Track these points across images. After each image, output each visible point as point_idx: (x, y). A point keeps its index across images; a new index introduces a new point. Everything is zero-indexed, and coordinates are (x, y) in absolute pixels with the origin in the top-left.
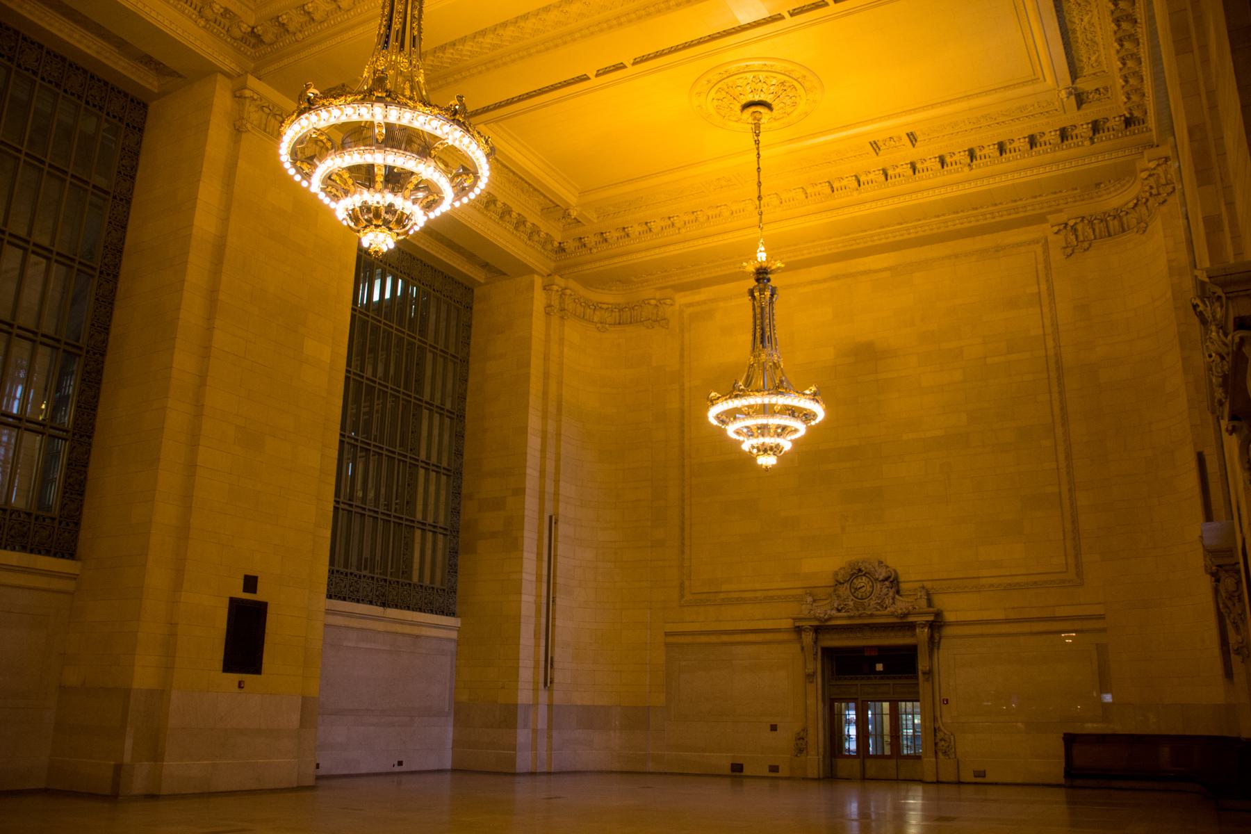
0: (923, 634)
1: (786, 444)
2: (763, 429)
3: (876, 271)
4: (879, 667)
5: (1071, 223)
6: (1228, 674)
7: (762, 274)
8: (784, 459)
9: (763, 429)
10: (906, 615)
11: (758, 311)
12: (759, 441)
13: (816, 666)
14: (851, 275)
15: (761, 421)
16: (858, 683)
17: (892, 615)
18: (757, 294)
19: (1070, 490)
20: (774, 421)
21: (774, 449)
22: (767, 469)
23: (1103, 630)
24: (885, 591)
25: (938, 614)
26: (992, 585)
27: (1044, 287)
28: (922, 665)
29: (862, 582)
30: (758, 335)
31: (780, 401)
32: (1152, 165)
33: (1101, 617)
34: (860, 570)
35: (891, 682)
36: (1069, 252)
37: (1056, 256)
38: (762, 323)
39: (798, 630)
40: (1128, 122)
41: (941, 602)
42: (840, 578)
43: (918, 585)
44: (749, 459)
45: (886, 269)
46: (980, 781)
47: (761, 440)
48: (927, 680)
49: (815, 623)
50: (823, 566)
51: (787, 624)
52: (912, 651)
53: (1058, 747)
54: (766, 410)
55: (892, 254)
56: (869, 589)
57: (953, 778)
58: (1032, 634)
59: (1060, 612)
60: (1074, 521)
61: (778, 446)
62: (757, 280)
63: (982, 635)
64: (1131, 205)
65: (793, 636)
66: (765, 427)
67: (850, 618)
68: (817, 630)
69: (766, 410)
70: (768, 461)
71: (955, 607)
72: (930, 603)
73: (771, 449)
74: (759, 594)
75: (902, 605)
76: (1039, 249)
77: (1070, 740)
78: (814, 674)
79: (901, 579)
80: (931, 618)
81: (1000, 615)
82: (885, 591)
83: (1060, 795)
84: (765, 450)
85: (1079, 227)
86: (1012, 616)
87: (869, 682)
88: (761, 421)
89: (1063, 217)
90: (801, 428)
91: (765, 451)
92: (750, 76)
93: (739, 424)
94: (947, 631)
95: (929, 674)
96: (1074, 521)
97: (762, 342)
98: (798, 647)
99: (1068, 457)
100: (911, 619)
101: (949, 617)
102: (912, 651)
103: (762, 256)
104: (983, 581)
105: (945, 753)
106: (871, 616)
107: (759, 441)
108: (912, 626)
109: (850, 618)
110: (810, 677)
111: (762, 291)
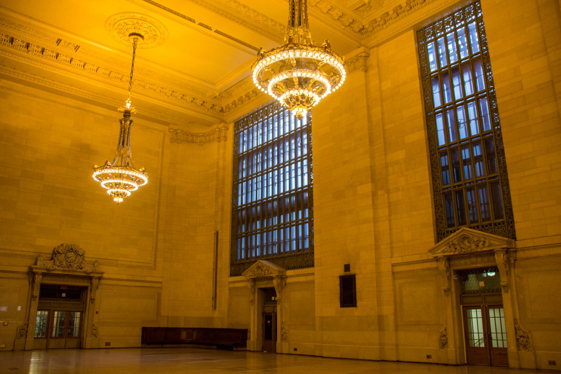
2: (117, 185)
3: (70, 106)
4: (64, 295)
5: (178, 131)
6: (215, 307)
7: (127, 114)
9: (117, 185)
10: (91, 273)
11: (123, 130)
12: (113, 190)
13: (37, 293)
14: (85, 110)
15: (118, 181)
16: (52, 302)
17: (85, 272)
18: (123, 122)
19: (157, 232)
20: (125, 182)
21: (118, 194)
22: (118, 204)
23: (161, 288)
24: (81, 260)
26: (123, 265)
27: (161, 151)
29: (71, 254)
30: (121, 141)
31: (106, 171)
32: (223, 128)
33: (161, 283)
34: (72, 249)
35: (69, 302)
36: (172, 141)
37: (167, 140)
38: (124, 136)
39: (31, 273)
40: (222, 111)
41: (102, 268)
42: (60, 251)
43: (94, 260)
45: (102, 115)
46: (108, 347)
47: (116, 190)
48: (92, 303)
49: (45, 271)
50: (48, 243)
51: (25, 269)
53: (139, 332)
54: (121, 176)
55: (106, 110)
56: (74, 258)
57: (97, 347)
58: (136, 286)
59: (148, 279)
60: (156, 244)
61: (124, 193)
62: (124, 116)
63: (116, 285)
64: (201, 135)
65: (26, 276)
66: (121, 184)
67: (64, 271)
68: (44, 275)
69: (121, 176)
71: (109, 272)
73: (121, 194)
74: (8, 252)
75: (88, 268)
76: (162, 135)
77: (144, 329)
78: (36, 297)
79: (85, 255)
81: (125, 277)
82: (81, 260)
83: (139, 351)
84: (118, 194)
85: (179, 134)
86: (130, 278)
87: (58, 302)
88: (118, 181)
89: (176, 127)
91: (118, 195)
92: (135, 21)
94: (102, 282)
95: (93, 300)
96: (156, 244)
97: (123, 144)
98: (26, 282)
99: (158, 219)
100: (92, 275)
101: (105, 276)
103: (128, 106)
104: (119, 262)
105: (95, 336)
106: (74, 271)
107: (113, 190)
108: (91, 278)
109: (64, 271)
110: (33, 297)
111: (126, 121)
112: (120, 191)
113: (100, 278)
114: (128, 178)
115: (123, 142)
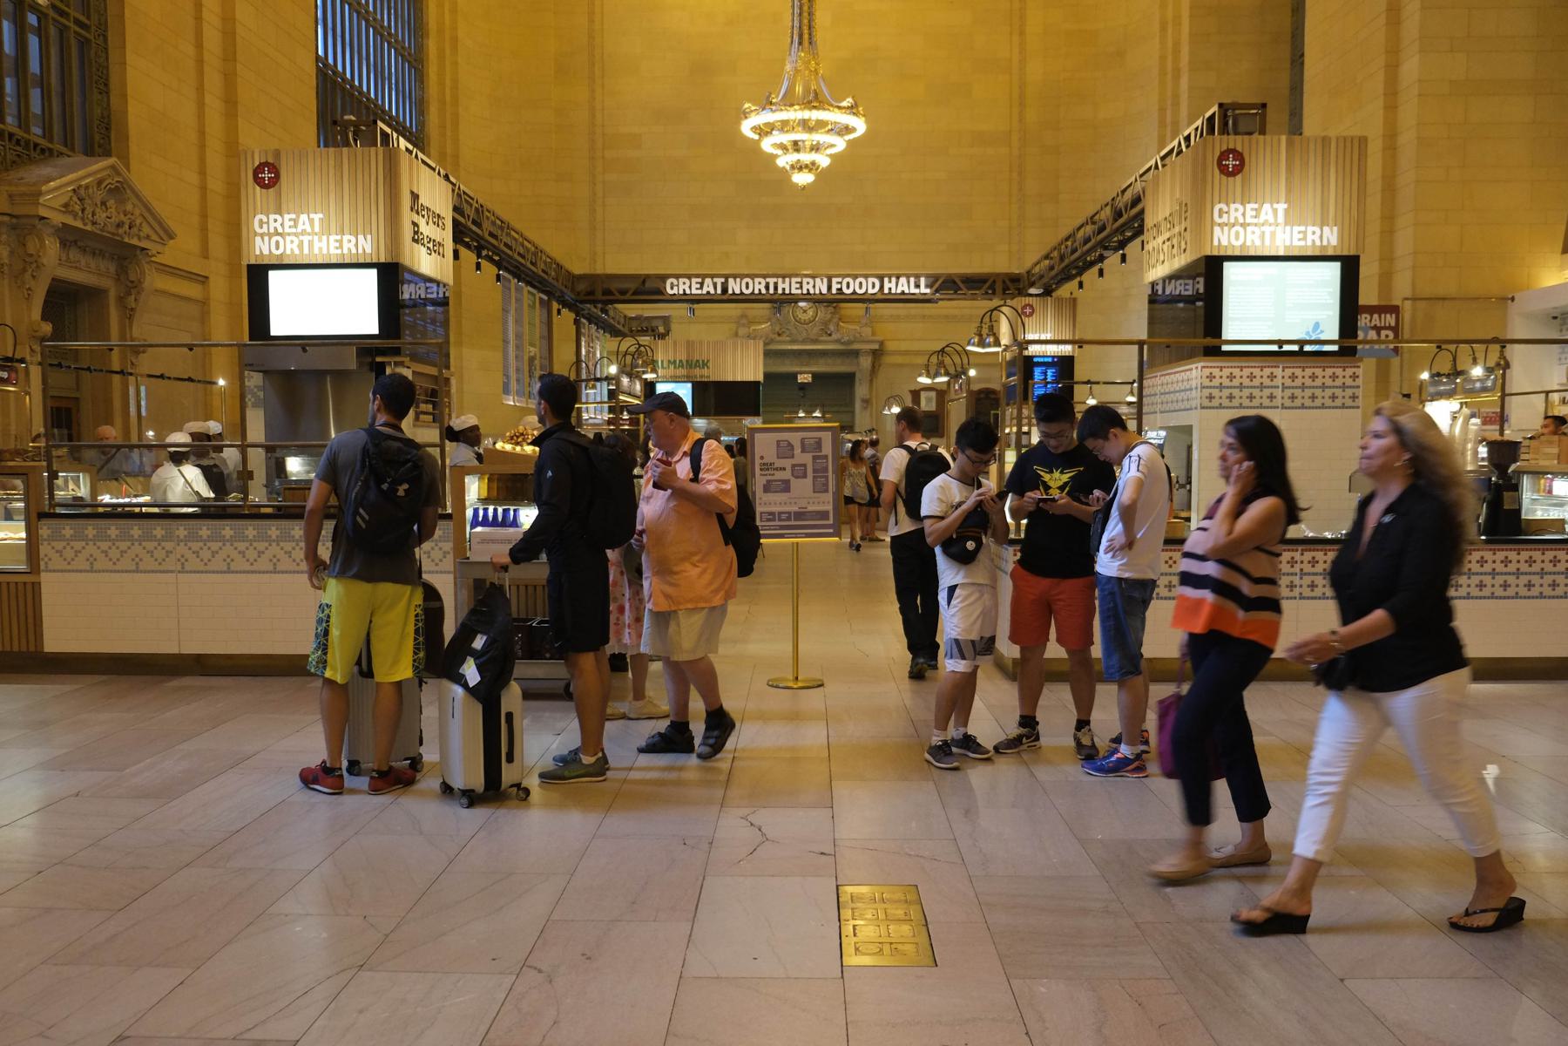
0: (865, 362)
1: (823, 161)
8: (823, 176)
12: (793, 157)
17: (838, 341)
21: (811, 167)
25: (882, 343)
28: (861, 391)
44: (784, 175)
52: (848, 379)
54: (806, 125)
69: (806, 125)
70: (803, 179)
72: (874, 334)
80: (876, 346)
90: (840, 144)
93: (786, 138)
94: (887, 359)
100: (856, 346)
101: (891, 346)
102: (848, 379)
112: (806, 157)
113: (877, 354)
114: (821, 124)
115: (801, 36)
